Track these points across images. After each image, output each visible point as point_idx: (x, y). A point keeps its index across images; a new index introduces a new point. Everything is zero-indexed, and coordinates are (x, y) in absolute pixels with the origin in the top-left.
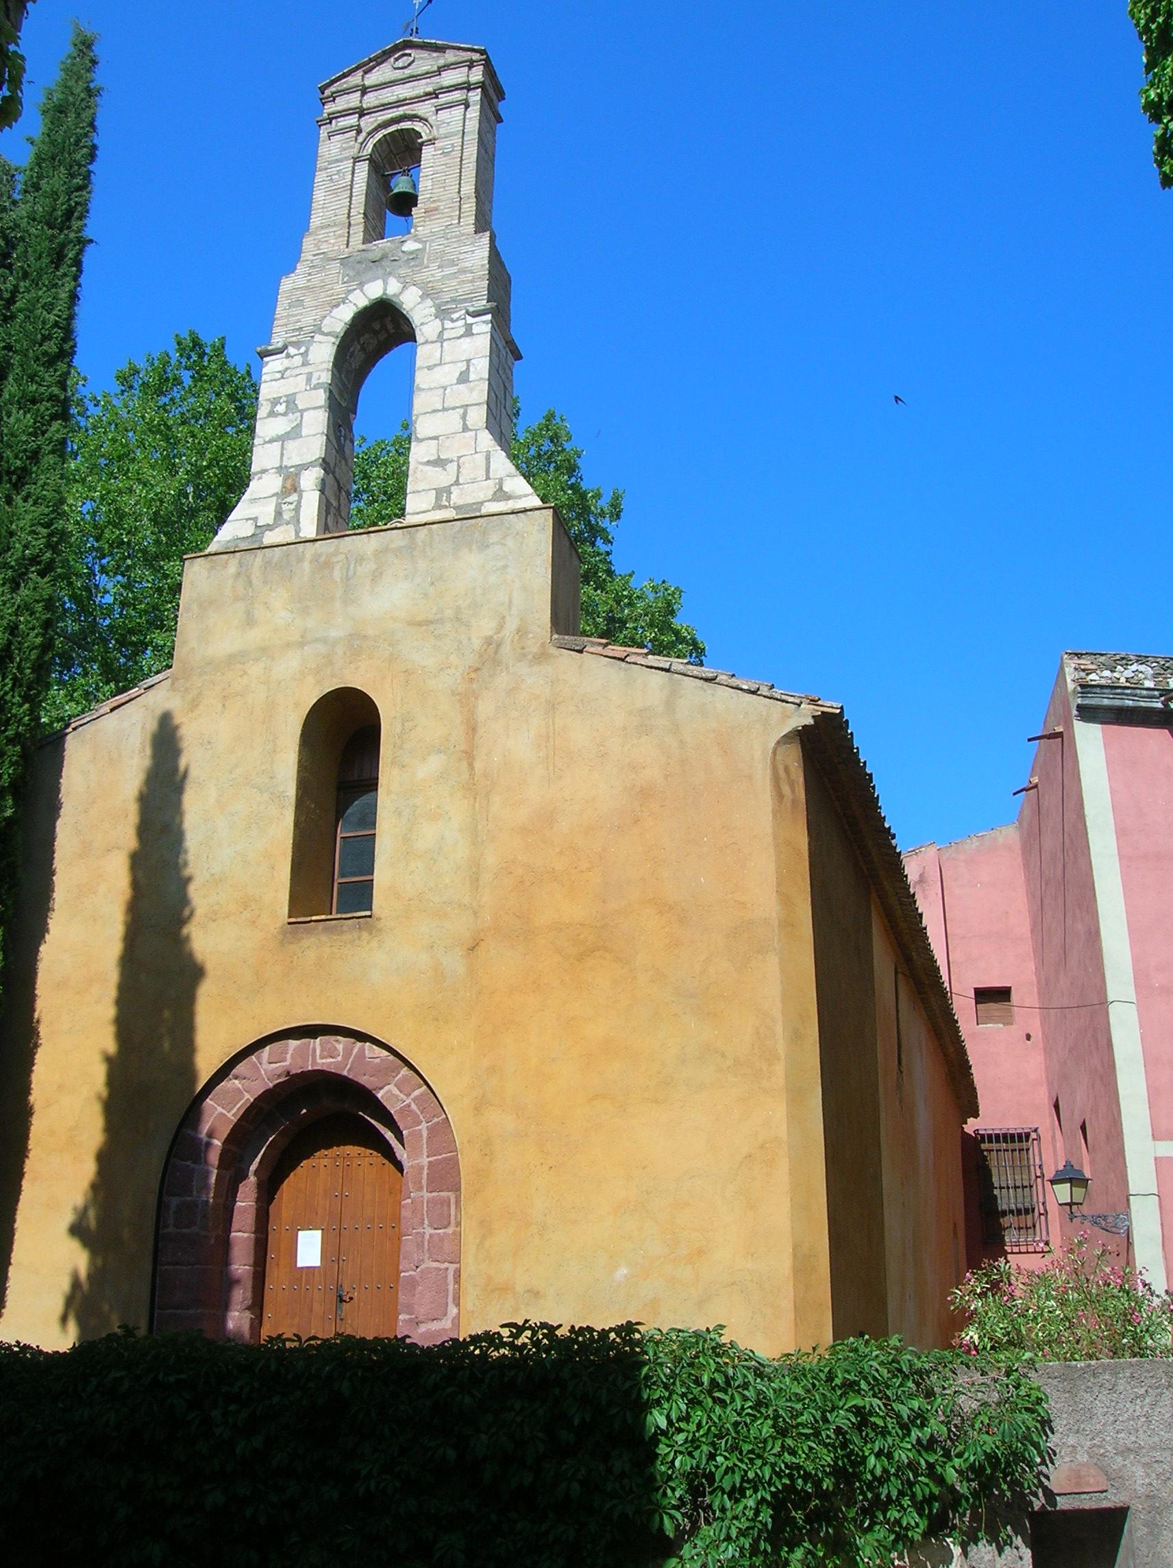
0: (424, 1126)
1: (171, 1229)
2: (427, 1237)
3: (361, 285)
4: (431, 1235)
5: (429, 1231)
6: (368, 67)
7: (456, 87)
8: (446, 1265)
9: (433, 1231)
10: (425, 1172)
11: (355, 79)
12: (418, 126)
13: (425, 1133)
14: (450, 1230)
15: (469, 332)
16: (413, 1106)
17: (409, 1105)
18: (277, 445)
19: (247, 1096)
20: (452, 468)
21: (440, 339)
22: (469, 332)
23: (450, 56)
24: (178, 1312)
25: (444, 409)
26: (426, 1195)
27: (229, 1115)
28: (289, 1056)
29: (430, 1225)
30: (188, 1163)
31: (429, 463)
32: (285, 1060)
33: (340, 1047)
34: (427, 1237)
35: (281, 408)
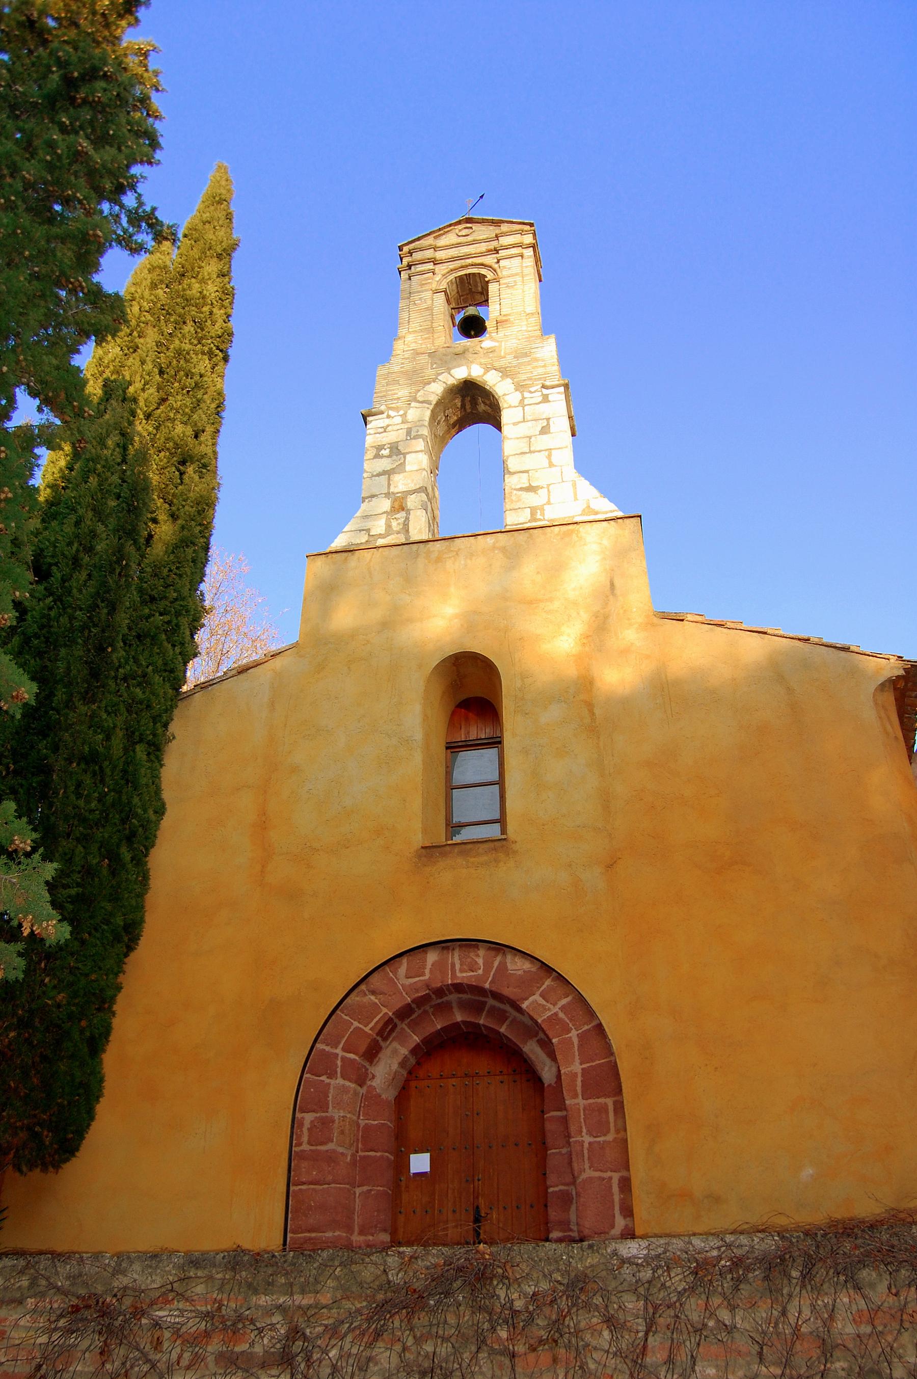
0: (574, 1034)
1: (305, 1147)
2: (586, 1145)
3: (448, 370)
4: (590, 1143)
5: (587, 1139)
6: (440, 232)
7: (514, 246)
8: (609, 1174)
9: (592, 1139)
10: (579, 1079)
11: (430, 241)
12: (483, 271)
13: (576, 1041)
14: (610, 1137)
15: (546, 399)
16: (561, 1015)
17: (556, 1014)
18: (384, 478)
19: (385, 1010)
20: (543, 493)
21: (522, 403)
22: (546, 399)
23: (505, 228)
24: (313, 1235)
25: (530, 452)
26: (581, 1102)
27: (367, 1029)
28: (427, 971)
29: (590, 1133)
30: (323, 1078)
31: (521, 489)
32: (423, 974)
33: (480, 961)
34: (586, 1145)
35: (385, 452)
